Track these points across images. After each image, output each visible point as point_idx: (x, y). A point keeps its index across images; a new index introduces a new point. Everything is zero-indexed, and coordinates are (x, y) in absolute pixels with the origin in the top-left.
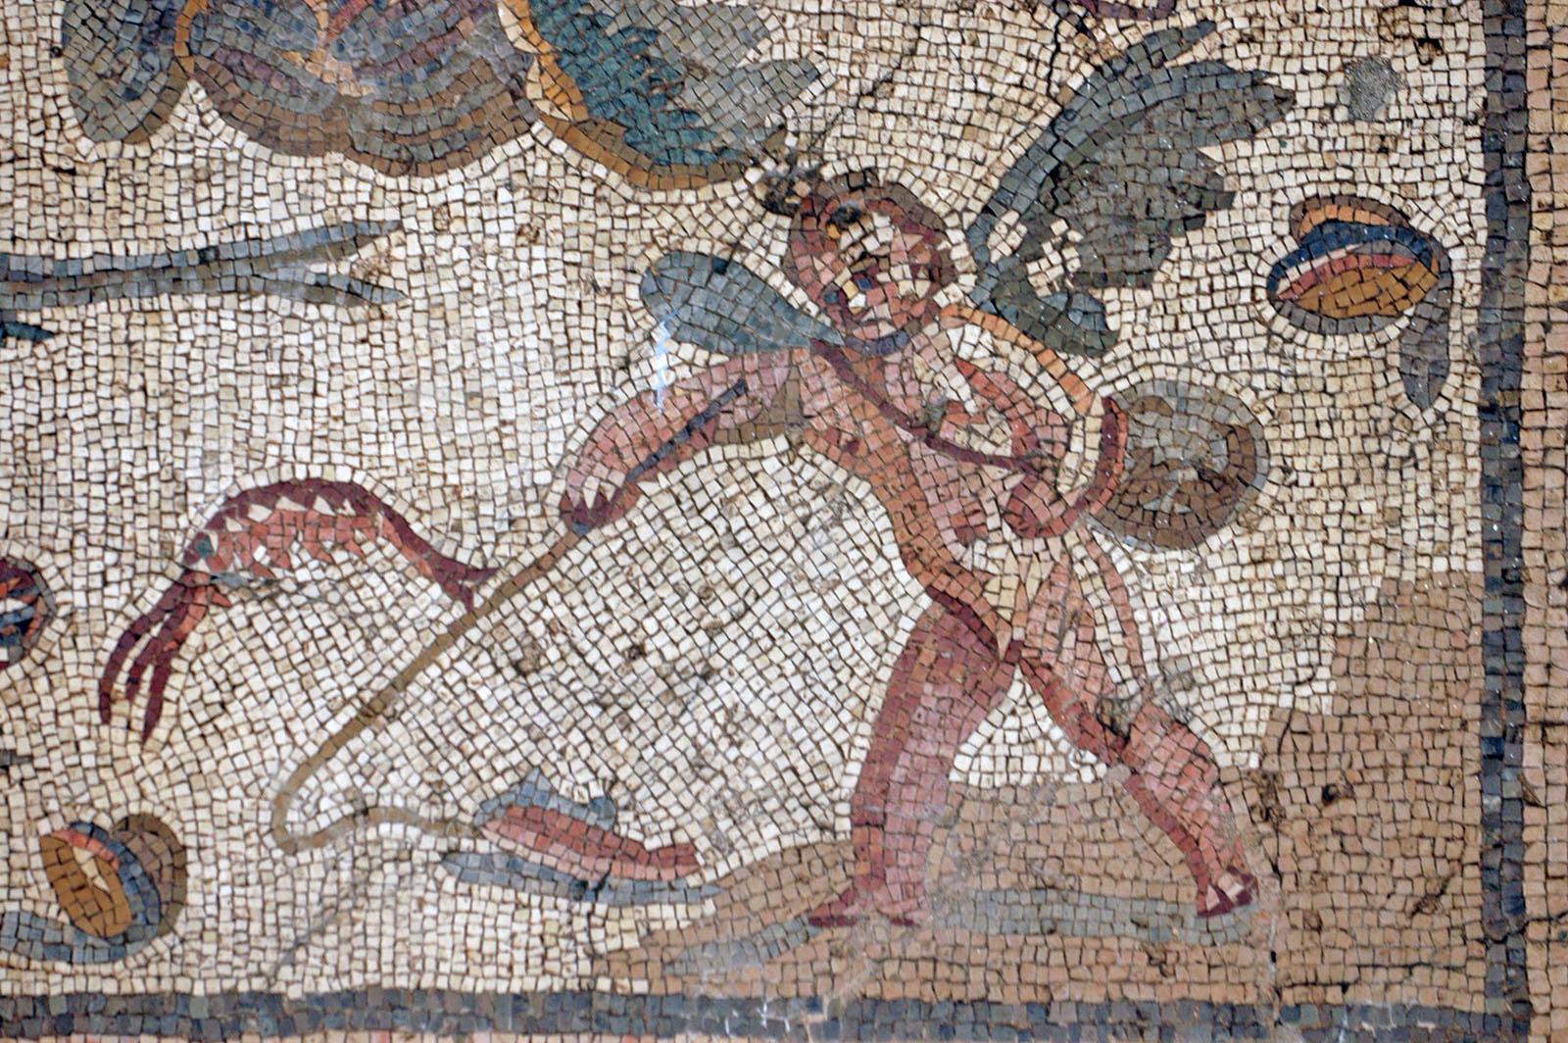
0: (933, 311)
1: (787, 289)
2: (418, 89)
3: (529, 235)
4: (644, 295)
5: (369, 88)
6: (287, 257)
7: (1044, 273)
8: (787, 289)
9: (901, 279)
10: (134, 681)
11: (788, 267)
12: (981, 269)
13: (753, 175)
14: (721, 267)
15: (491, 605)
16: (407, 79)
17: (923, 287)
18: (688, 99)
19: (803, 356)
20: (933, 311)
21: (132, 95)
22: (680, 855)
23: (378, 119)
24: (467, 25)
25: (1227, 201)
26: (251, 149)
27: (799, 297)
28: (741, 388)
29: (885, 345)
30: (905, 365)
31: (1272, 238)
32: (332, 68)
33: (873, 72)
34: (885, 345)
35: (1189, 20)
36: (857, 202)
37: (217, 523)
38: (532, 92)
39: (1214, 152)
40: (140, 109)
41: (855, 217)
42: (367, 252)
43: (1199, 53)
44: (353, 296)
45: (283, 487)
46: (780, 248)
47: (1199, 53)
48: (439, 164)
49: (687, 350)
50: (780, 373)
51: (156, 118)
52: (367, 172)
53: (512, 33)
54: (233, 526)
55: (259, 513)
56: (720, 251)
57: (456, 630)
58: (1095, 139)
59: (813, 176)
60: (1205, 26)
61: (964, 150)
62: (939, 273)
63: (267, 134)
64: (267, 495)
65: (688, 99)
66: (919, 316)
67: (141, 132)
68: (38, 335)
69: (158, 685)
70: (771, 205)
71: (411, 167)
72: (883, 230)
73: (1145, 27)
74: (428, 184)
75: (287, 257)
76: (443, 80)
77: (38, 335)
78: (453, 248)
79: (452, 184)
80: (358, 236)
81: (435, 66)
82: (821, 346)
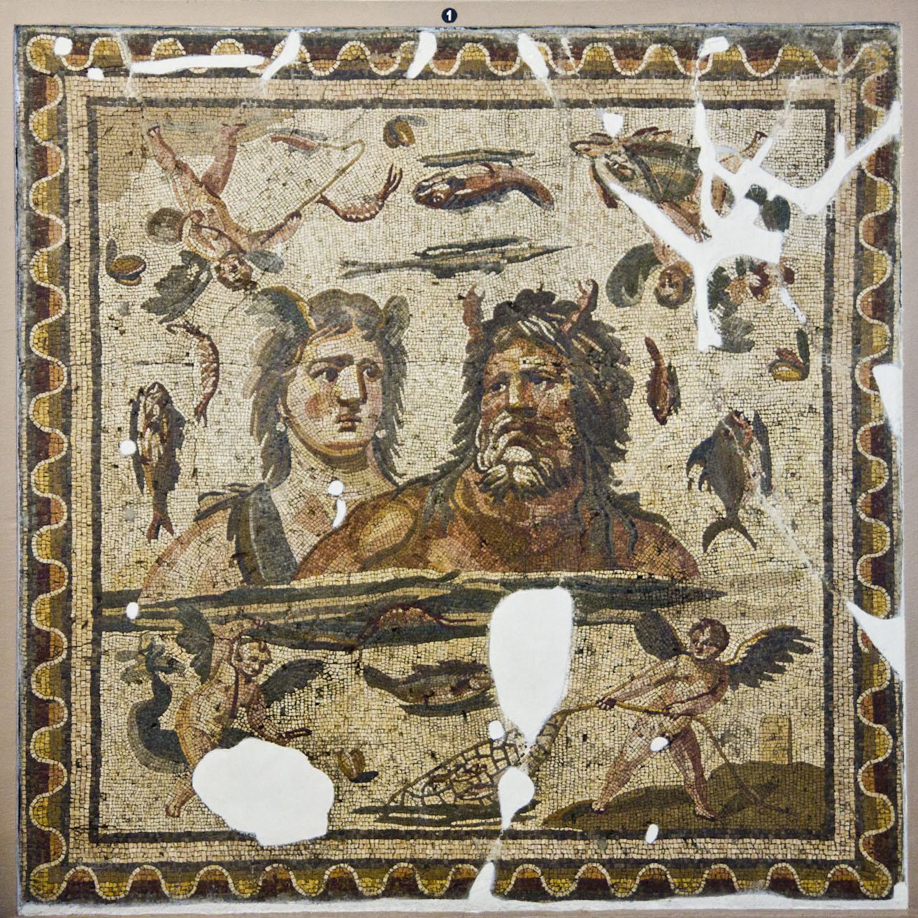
0: (220, 260)
1: (252, 265)
2: (333, 308)
3: (308, 277)
4: (283, 263)
5: (344, 308)
6: (361, 271)
7: (195, 269)
8: (252, 265)
9: (226, 267)
10: (395, 177)
11: (252, 270)
12: (209, 270)
13: (259, 290)
14: (266, 270)
15: (316, 195)
16: (335, 310)
17: (222, 265)
18: (274, 307)
19: (248, 250)
20: (220, 260)
21: (395, 306)
22: (275, 139)
23: (342, 302)
24: (322, 322)
25: (156, 285)
26: (369, 295)
27: (249, 263)
28: (262, 243)
29: (230, 253)
30: (226, 248)
31: (145, 276)
32: (352, 312)
33: (233, 312)
34: (230, 253)
35: (164, 324)
36: (237, 284)
37: (377, 213)
38: (308, 308)
39: (159, 295)
40: (393, 303)
41: (237, 281)
42: (344, 272)
43: (162, 317)
44: (347, 263)
45: (362, 221)
46: (253, 274)
47: (162, 317)
48: (328, 292)
49: (274, 251)
50: (253, 247)
51: (390, 301)
52: (344, 290)
53: (312, 321)
54: (373, 212)
55: (368, 215)
56: (267, 273)
57: (324, 189)
58: (184, 298)
59: (246, 290)
60: (161, 322)
61: (213, 296)
62: (218, 269)
63: (366, 298)
64: (366, 219)
65: (274, 307)
66: (223, 259)
67: (393, 298)
68: (416, 254)
69: (390, 177)
70: (255, 283)
71: (334, 291)
72: (231, 278)
73: (174, 322)
74: (331, 288)
75: (361, 271)
76: (328, 310)
77: (416, 254)
78: (325, 273)
79: (325, 288)
80: (346, 276)
81: (330, 313)
82: (245, 253)
